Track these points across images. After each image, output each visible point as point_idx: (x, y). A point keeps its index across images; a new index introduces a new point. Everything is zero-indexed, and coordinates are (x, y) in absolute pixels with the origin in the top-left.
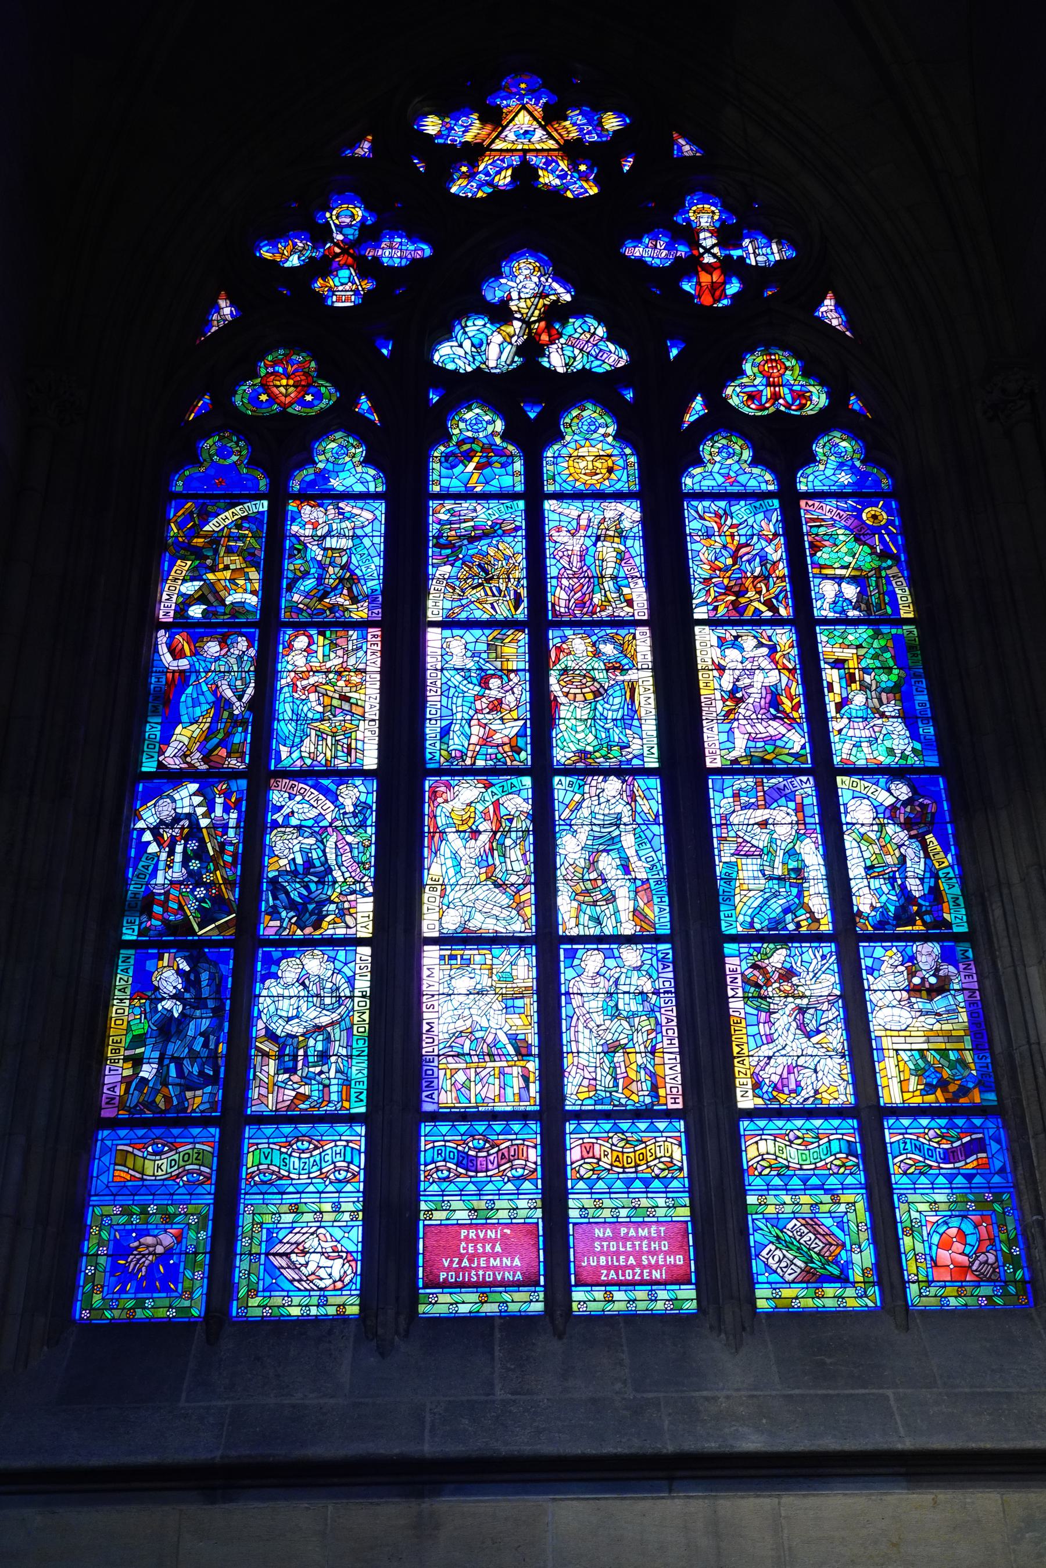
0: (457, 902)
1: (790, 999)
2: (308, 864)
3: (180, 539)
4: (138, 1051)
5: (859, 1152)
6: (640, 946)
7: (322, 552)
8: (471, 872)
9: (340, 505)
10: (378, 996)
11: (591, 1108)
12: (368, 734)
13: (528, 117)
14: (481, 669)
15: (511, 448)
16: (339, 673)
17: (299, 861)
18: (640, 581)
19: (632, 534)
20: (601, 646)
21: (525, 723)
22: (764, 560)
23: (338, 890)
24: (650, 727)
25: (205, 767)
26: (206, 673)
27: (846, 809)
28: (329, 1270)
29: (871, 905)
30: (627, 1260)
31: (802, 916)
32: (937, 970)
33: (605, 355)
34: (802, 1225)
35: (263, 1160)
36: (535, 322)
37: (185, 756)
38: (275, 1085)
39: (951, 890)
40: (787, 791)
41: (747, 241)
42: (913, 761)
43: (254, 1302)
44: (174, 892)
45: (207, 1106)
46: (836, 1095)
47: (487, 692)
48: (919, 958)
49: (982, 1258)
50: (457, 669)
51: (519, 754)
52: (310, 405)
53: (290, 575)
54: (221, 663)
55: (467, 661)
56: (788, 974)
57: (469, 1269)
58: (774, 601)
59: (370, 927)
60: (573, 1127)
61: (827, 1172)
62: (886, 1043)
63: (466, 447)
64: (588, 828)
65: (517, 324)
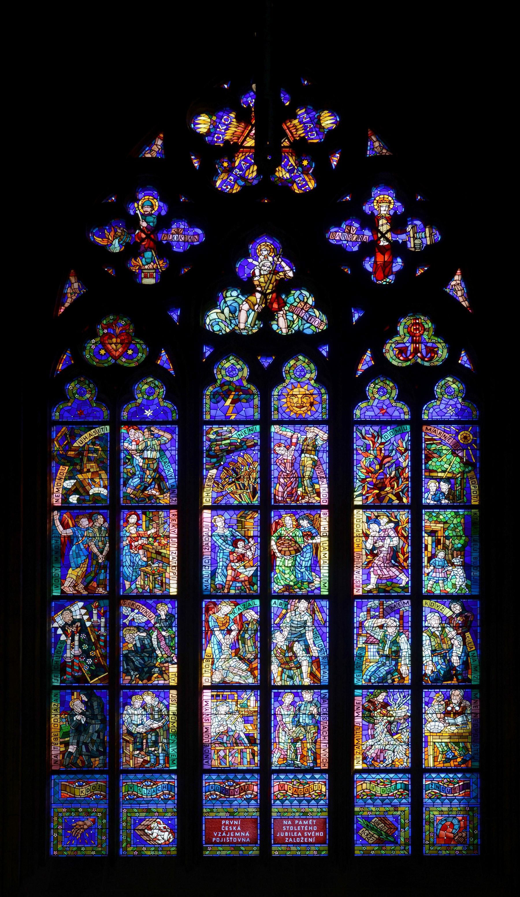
1: (385, 718)
2: (143, 646)
3: (61, 452)
4: (66, 739)
6: (312, 691)
7: (142, 461)
8: (227, 651)
9: (152, 429)
10: (181, 714)
12: (171, 574)
15: (253, 388)
16: (155, 539)
17: (138, 645)
19: (322, 449)
20: (301, 522)
21: (257, 569)
22: (397, 464)
23: (159, 661)
24: (325, 571)
25: (86, 593)
26: (82, 537)
27: (426, 618)
29: (432, 670)
30: (297, 834)
31: (396, 675)
33: (313, 319)
35: (130, 789)
36: (269, 294)
37: (75, 586)
39: (474, 662)
40: (396, 609)
41: (410, 226)
42: (466, 591)
43: (130, 849)
44: (76, 661)
45: (102, 765)
46: (402, 763)
47: (236, 549)
49: (460, 835)
50: (219, 536)
51: (253, 586)
52: (130, 357)
53: (125, 476)
55: (225, 530)
56: (385, 705)
57: (226, 837)
59: (176, 680)
60: (275, 777)
62: (430, 739)
63: (226, 388)
64: (289, 629)
65: (258, 295)
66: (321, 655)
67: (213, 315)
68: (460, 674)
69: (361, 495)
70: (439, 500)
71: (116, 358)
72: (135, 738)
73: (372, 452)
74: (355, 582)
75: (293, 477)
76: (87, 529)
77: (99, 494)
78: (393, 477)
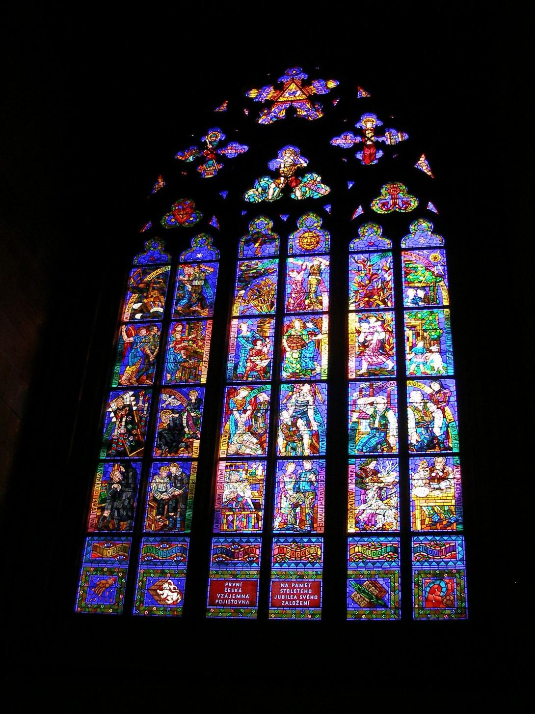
0: (235, 441)
1: (376, 484)
4: (103, 505)
5: (399, 551)
8: (242, 428)
11: (285, 532)
12: (203, 367)
13: (295, 86)
14: (254, 337)
17: (171, 424)
18: (326, 293)
19: (325, 272)
21: (271, 361)
23: (186, 437)
26: (140, 343)
27: (410, 396)
28: (172, 597)
30: (293, 597)
32: (444, 469)
34: (370, 583)
37: (130, 379)
38: (155, 520)
41: (387, 133)
45: (128, 528)
46: (391, 526)
47: (255, 347)
48: (436, 465)
49: (448, 598)
51: (267, 375)
54: (146, 338)
56: (376, 472)
57: (227, 599)
58: (386, 300)
61: (384, 560)
62: (417, 503)
64: (294, 407)
65: (282, 179)
66: (320, 429)
67: (251, 192)
68: (441, 443)
69: (355, 302)
70: (417, 303)
71: (181, 223)
72: (159, 504)
73: (363, 272)
74: (349, 368)
75: (302, 292)
76: (145, 337)
77: (157, 312)
78: (380, 288)
